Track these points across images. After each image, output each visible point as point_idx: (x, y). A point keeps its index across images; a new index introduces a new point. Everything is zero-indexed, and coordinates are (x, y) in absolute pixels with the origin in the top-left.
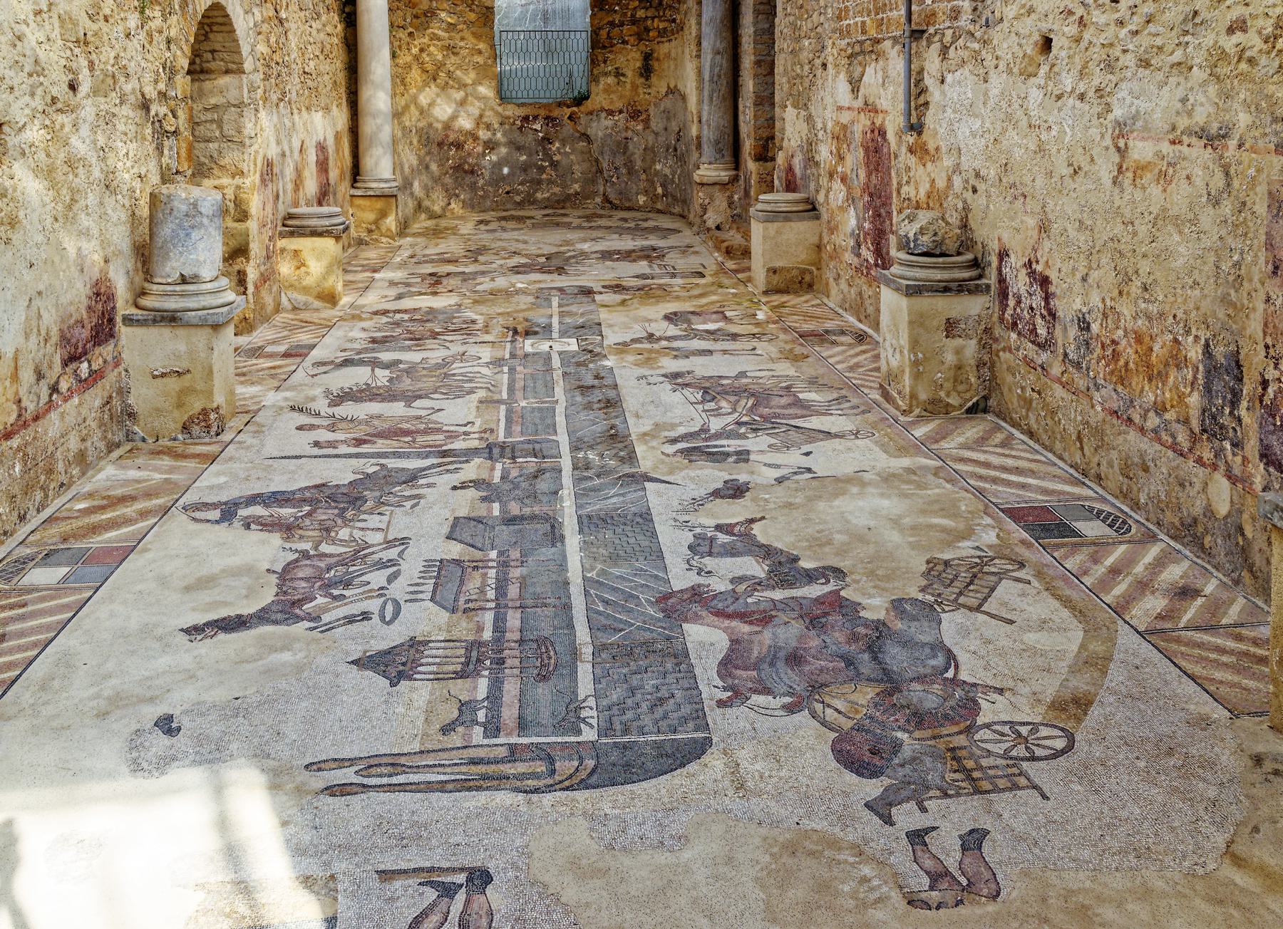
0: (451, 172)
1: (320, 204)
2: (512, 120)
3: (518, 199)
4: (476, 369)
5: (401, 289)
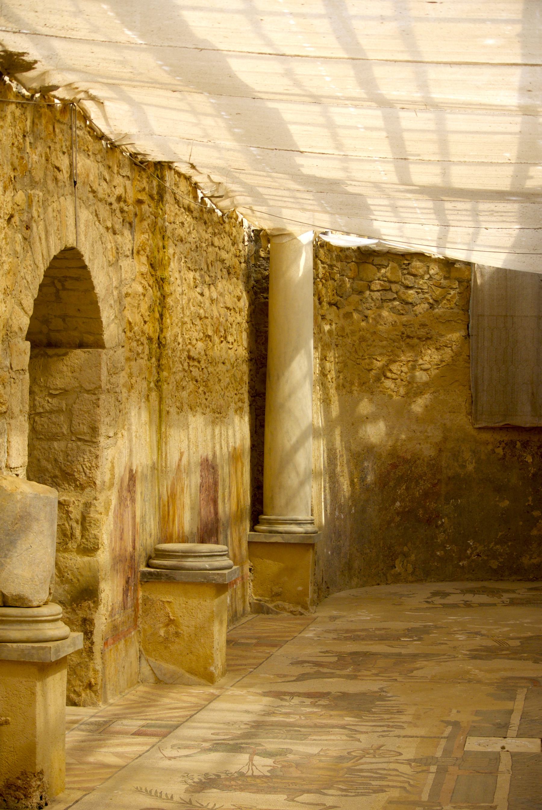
0: (398, 519)
1: (202, 541)
2: (490, 447)
3: (494, 564)
4: (392, 766)
5: (308, 669)
